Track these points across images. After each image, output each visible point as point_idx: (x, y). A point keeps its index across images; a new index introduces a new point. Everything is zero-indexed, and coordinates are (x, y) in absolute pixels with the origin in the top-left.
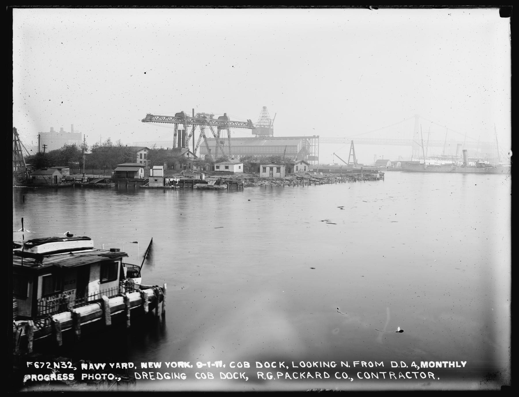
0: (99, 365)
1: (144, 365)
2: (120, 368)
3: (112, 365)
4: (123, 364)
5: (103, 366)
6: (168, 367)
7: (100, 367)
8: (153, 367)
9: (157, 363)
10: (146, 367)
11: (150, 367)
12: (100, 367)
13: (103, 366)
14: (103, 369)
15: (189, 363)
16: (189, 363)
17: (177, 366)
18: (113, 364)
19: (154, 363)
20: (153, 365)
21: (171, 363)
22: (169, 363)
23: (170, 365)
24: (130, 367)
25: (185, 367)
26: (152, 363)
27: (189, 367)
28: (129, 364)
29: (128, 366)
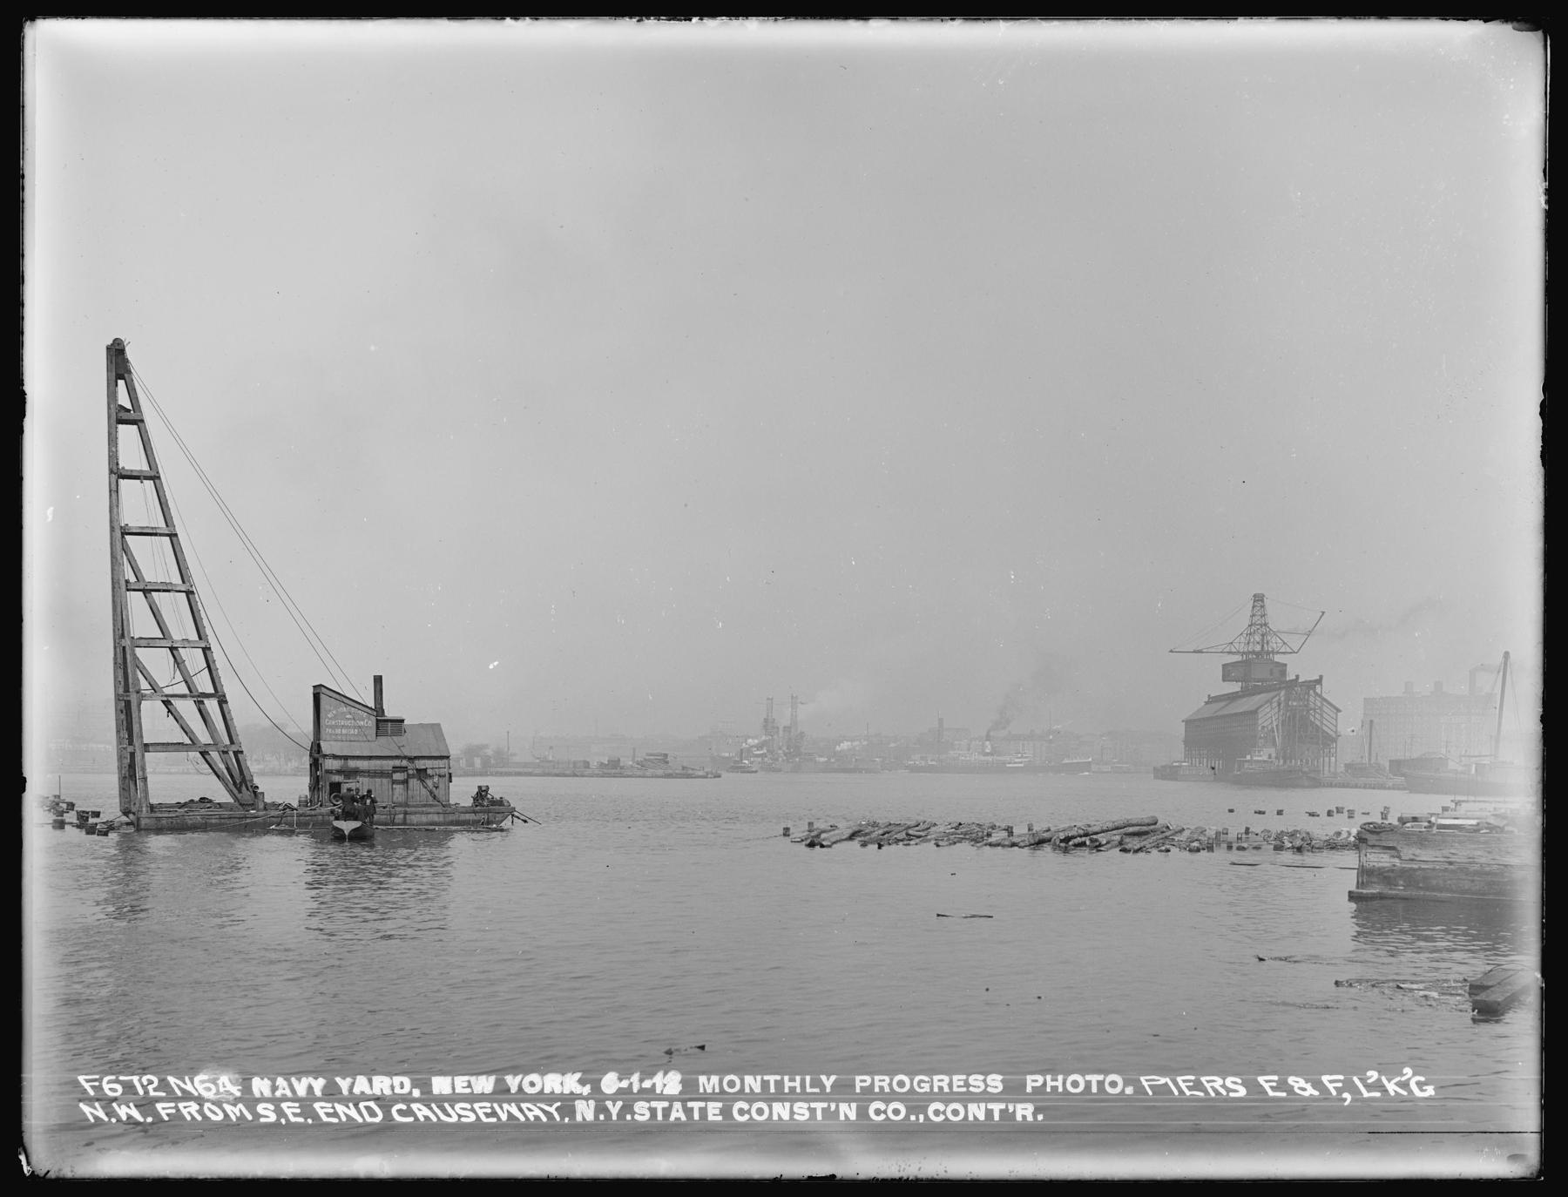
0: (305, 1081)
1: (441, 1085)
2: (368, 1091)
3: (344, 1084)
4: (376, 1079)
5: (319, 1084)
6: (514, 1090)
7: (310, 1088)
8: (468, 1091)
9: (483, 1078)
10: (447, 1090)
11: (457, 1091)
12: (310, 1088)
13: (319, 1084)
14: (318, 1093)
15: (578, 1076)
16: (578, 1076)
17: (543, 1089)
18: (349, 1080)
19: (473, 1079)
20: (470, 1086)
21: (523, 1079)
22: (519, 1077)
23: (520, 1089)
24: (398, 1090)
25: (566, 1091)
26: (466, 1078)
27: (578, 1089)
28: (397, 1080)
29: (392, 1088)
